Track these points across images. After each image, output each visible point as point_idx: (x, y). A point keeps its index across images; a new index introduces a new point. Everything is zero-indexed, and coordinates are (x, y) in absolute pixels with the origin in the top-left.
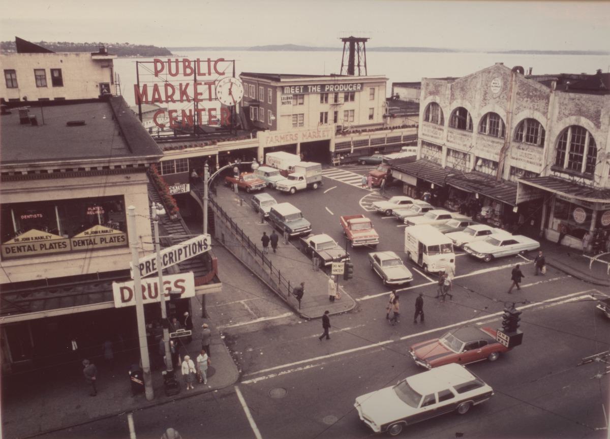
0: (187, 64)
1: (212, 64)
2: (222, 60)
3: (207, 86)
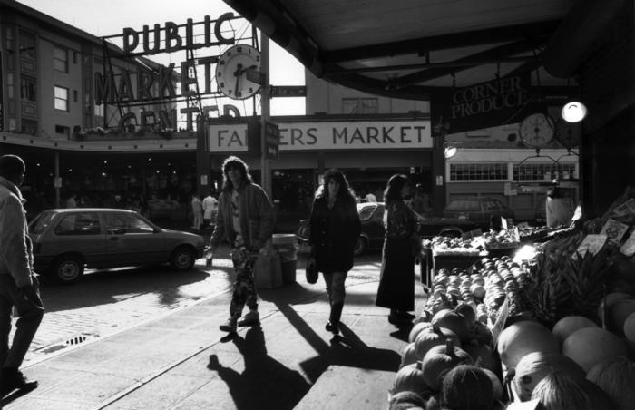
0: (172, 31)
1: (213, 25)
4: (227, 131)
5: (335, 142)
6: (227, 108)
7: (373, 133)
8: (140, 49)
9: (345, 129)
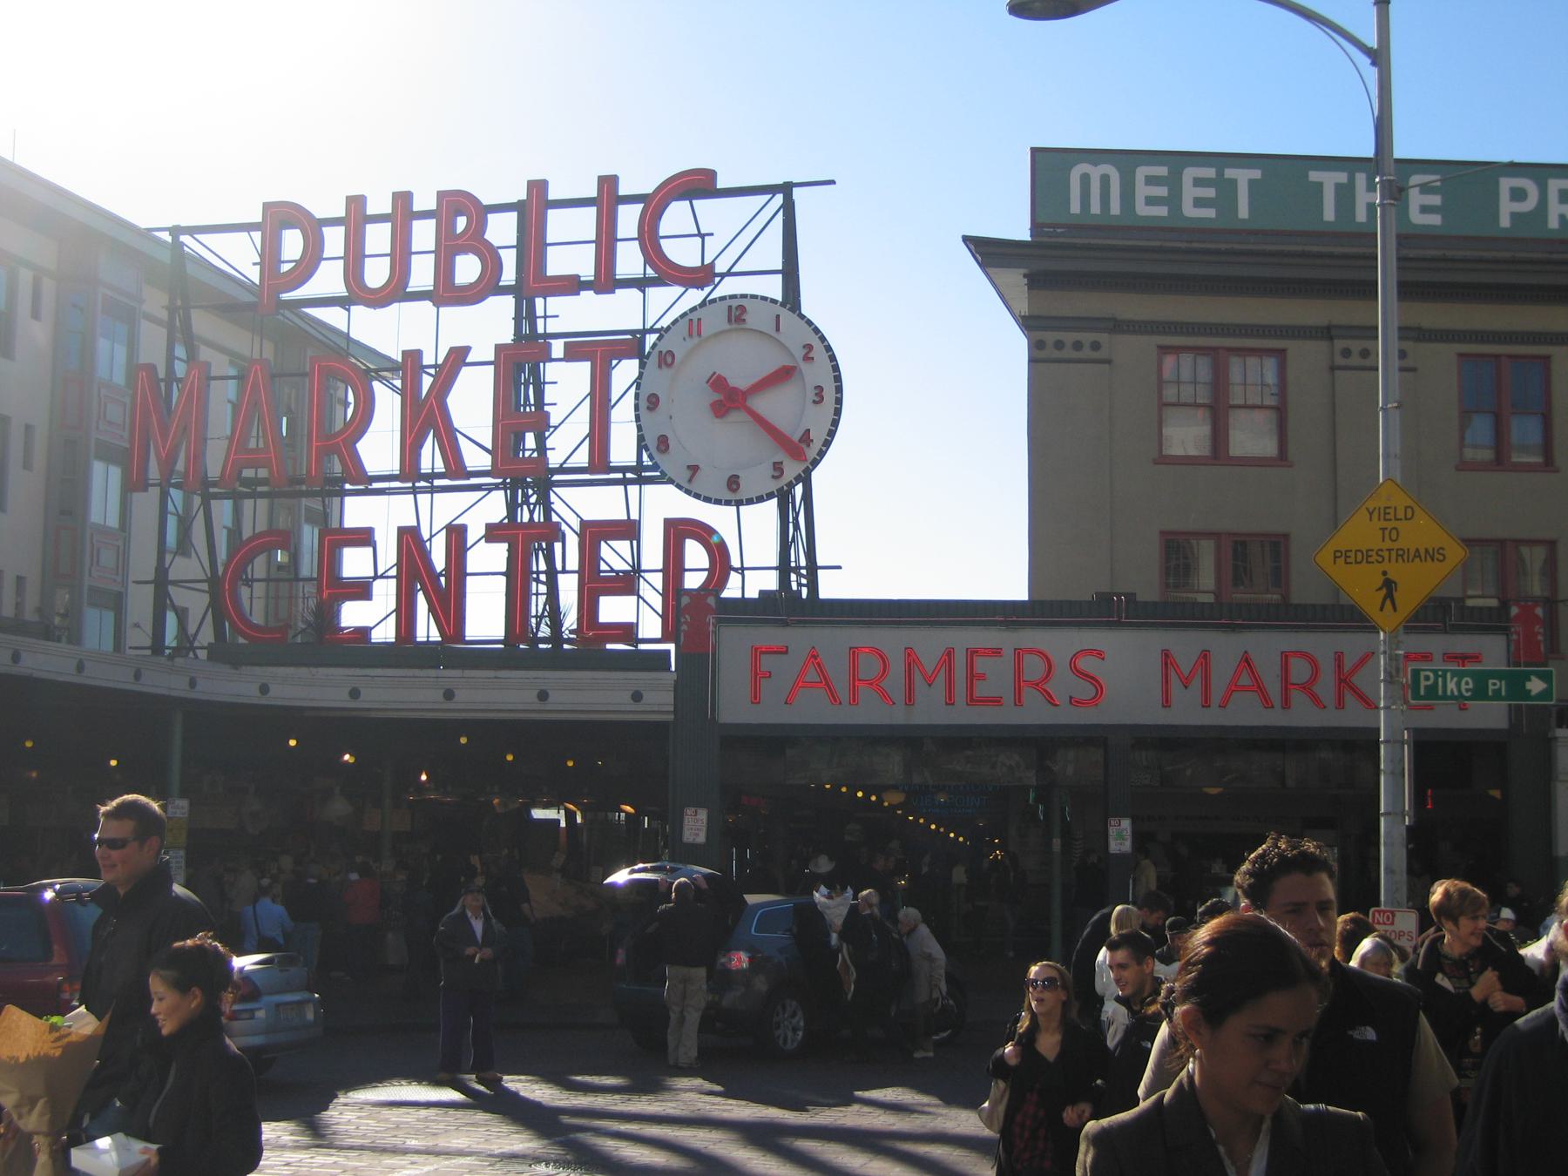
0: (461, 223)
1: (628, 219)
2: (697, 185)
3: (584, 369)
4: (784, 651)
5: (1166, 703)
6: (678, 532)
7: (1300, 670)
8: (329, 279)
9: (1205, 656)
